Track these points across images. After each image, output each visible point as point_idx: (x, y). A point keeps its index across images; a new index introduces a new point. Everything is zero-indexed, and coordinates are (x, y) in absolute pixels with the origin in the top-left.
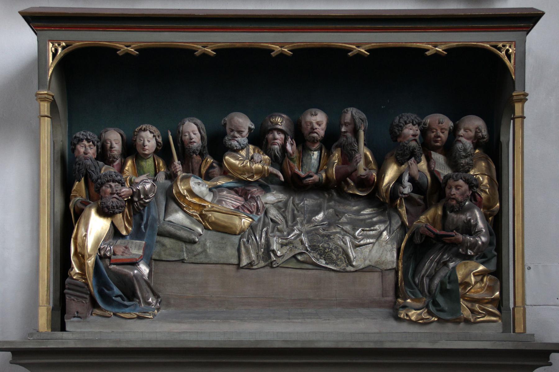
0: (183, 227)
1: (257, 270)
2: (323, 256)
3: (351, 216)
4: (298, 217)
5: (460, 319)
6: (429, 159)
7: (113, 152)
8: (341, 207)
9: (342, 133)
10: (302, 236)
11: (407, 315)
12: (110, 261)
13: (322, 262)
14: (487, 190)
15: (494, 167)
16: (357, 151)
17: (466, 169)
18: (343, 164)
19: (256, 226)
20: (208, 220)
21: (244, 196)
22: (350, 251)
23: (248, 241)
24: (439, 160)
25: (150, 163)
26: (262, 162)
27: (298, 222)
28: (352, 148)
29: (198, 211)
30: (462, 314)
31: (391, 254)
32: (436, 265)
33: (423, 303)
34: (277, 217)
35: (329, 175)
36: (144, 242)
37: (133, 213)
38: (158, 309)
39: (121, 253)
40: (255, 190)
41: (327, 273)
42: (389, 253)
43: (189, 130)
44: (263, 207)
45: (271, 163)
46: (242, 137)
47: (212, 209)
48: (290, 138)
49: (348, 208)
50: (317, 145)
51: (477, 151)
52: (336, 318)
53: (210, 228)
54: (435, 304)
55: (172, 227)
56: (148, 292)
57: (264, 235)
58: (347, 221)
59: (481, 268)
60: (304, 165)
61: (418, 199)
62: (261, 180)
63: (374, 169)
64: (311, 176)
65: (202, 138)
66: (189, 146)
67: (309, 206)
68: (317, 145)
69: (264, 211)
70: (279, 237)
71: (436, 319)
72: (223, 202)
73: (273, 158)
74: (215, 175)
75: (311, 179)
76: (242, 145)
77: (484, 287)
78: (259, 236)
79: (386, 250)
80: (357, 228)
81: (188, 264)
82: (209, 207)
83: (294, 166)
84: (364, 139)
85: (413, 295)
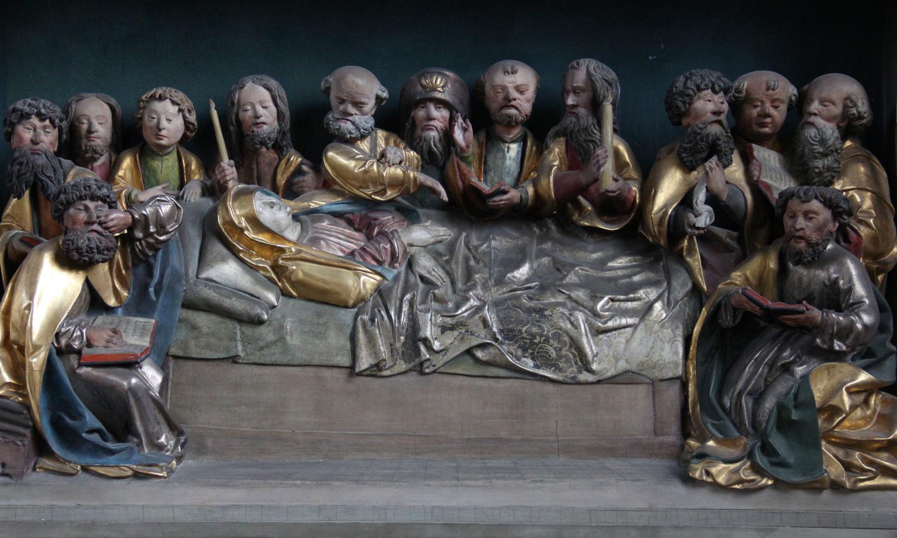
0: (238, 292)
1: (390, 379)
2: (530, 351)
3: (586, 271)
4: (477, 273)
5: (821, 481)
6: (747, 159)
7: (93, 141)
8: (566, 254)
9: (568, 109)
10: (486, 311)
11: (708, 473)
12: (79, 359)
13: (526, 364)
14: (871, 221)
15: (885, 174)
16: (599, 144)
17: (826, 180)
18: (570, 168)
19: (390, 290)
20: (290, 278)
21: (364, 231)
22: (585, 340)
23: (372, 320)
24: (770, 161)
25: (170, 164)
26: (403, 164)
27: (476, 282)
28: (589, 138)
29: (269, 260)
30: (826, 472)
31: (671, 347)
32: (766, 371)
33: (741, 448)
34: (433, 273)
35: (541, 191)
36: (154, 321)
37: (133, 263)
38: (179, 459)
39: (104, 343)
40: (388, 219)
41: (538, 385)
42: (667, 347)
43: (254, 99)
44: (405, 252)
45: (422, 165)
46: (363, 114)
47: (298, 256)
49: (581, 254)
50: (516, 132)
51: (848, 143)
52: (558, 478)
53: (294, 293)
54: (768, 450)
55: (214, 291)
56: (158, 423)
57: (405, 308)
58: (578, 281)
59: (864, 377)
60: (490, 170)
61: (726, 238)
62: (400, 199)
63: (635, 180)
64: (505, 192)
65: (280, 116)
66: (253, 132)
67: (500, 251)
68: (516, 132)
69: (406, 261)
70: (437, 312)
71: (770, 482)
72: (322, 242)
73: (426, 157)
74: (306, 189)
75: (505, 197)
76: (362, 130)
77: (871, 418)
78: (395, 311)
79: (661, 340)
80: (599, 295)
81: (246, 366)
82: (291, 252)
83: (470, 172)
84: (614, 119)
85: (721, 433)
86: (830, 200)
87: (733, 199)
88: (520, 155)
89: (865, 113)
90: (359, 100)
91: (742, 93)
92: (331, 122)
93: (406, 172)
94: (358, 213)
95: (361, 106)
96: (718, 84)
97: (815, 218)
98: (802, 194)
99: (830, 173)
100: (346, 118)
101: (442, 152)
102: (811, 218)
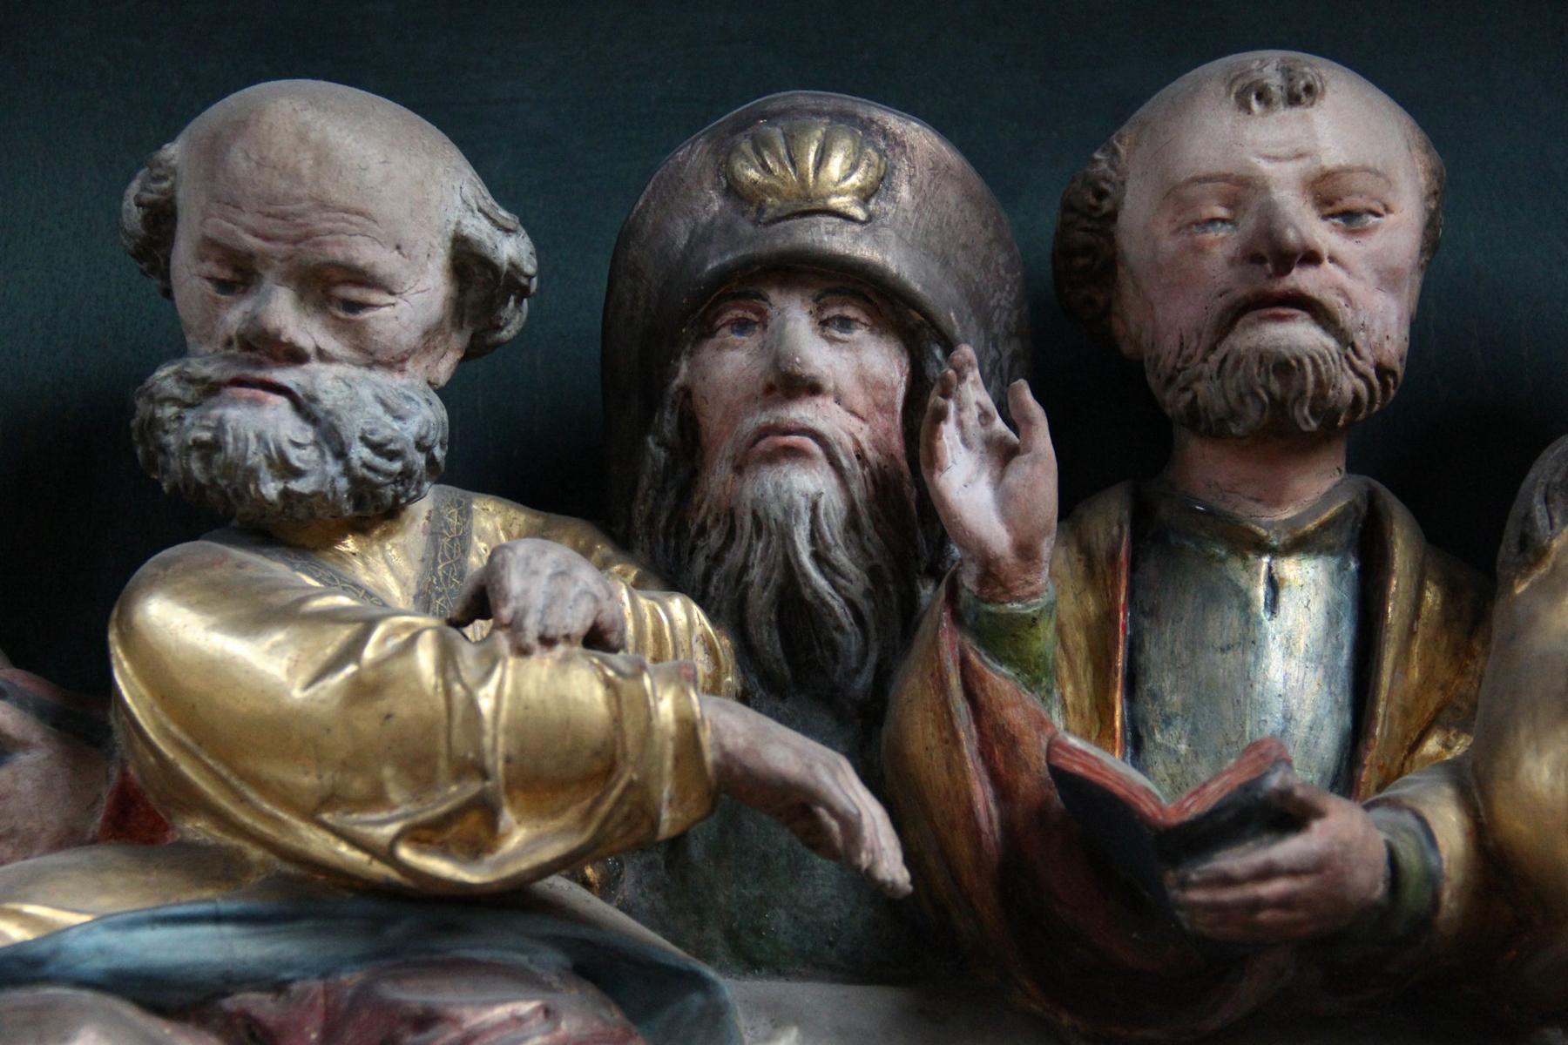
35: (1514, 824)
46: (375, 358)
48: (974, 375)
73: (768, 639)
75: (1290, 849)
88: (1346, 630)
90: (338, 254)
92: (170, 411)
93: (626, 686)
94: (317, 985)
95: (355, 293)
100: (261, 374)
101: (866, 607)
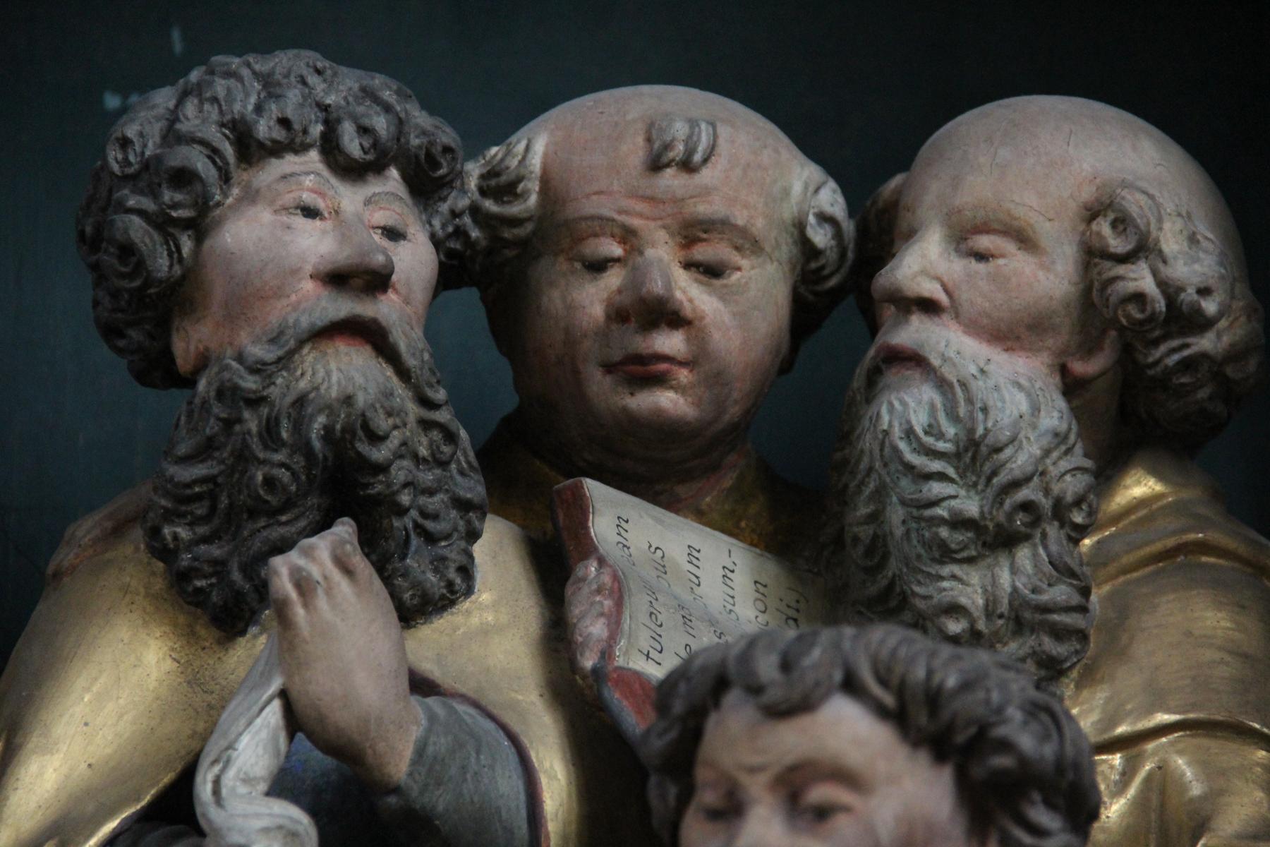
86: (934, 698)
87: (453, 771)
89: (1204, 292)
91: (523, 196)
96: (355, 119)
97: (846, 809)
98: (767, 667)
99: (1030, 642)
102: (823, 813)
